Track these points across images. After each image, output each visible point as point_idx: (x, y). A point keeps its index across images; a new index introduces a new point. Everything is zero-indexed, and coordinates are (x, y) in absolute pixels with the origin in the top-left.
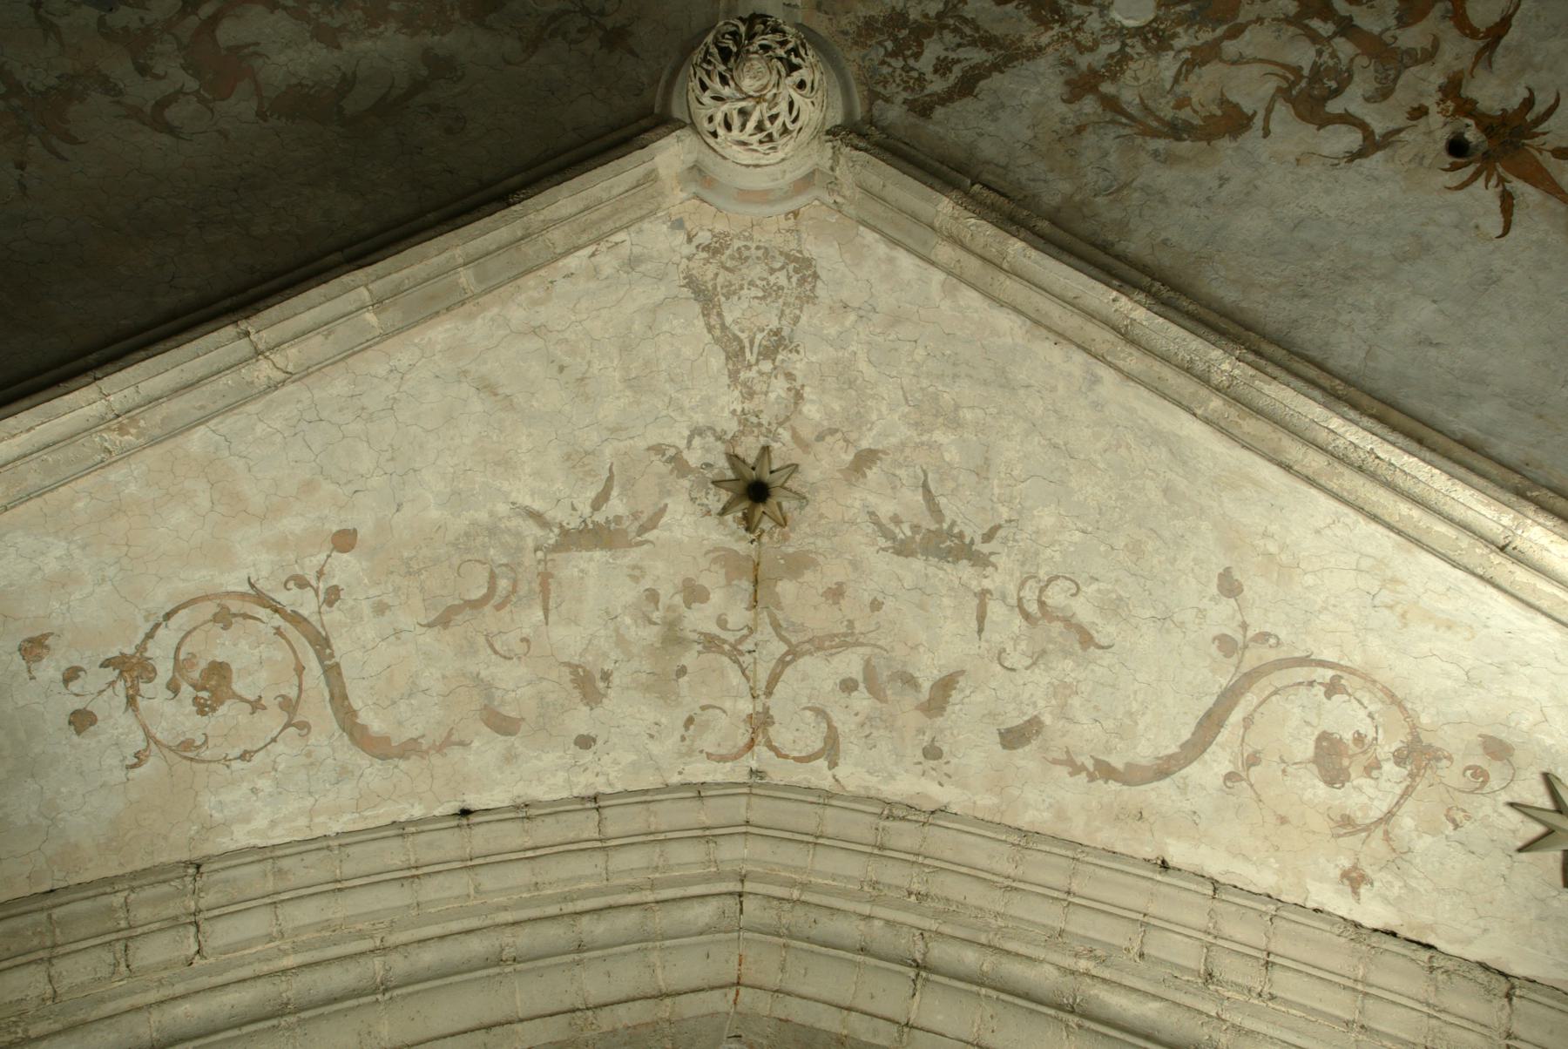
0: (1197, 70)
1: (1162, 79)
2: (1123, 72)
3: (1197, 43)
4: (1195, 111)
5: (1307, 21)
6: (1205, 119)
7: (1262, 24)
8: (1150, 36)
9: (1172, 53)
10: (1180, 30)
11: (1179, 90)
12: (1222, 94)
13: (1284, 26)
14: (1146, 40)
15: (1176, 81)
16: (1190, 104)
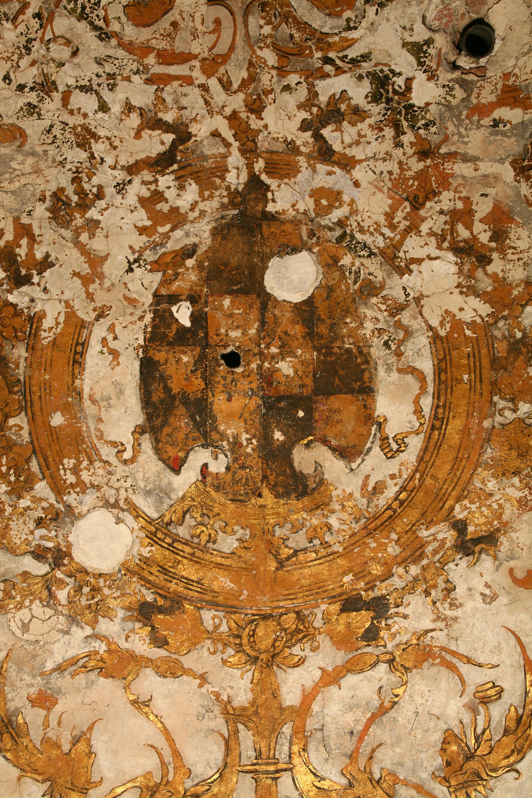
0: (93, 675)
1: (51, 652)
2: (20, 606)
3: (124, 645)
4: (46, 725)
5: (241, 727)
6: (45, 740)
7: (201, 686)
8: (86, 590)
9: (88, 631)
10: (121, 613)
11: (57, 681)
12: (90, 729)
13: (217, 710)
14: (79, 590)
15: (60, 669)
16: (49, 710)
